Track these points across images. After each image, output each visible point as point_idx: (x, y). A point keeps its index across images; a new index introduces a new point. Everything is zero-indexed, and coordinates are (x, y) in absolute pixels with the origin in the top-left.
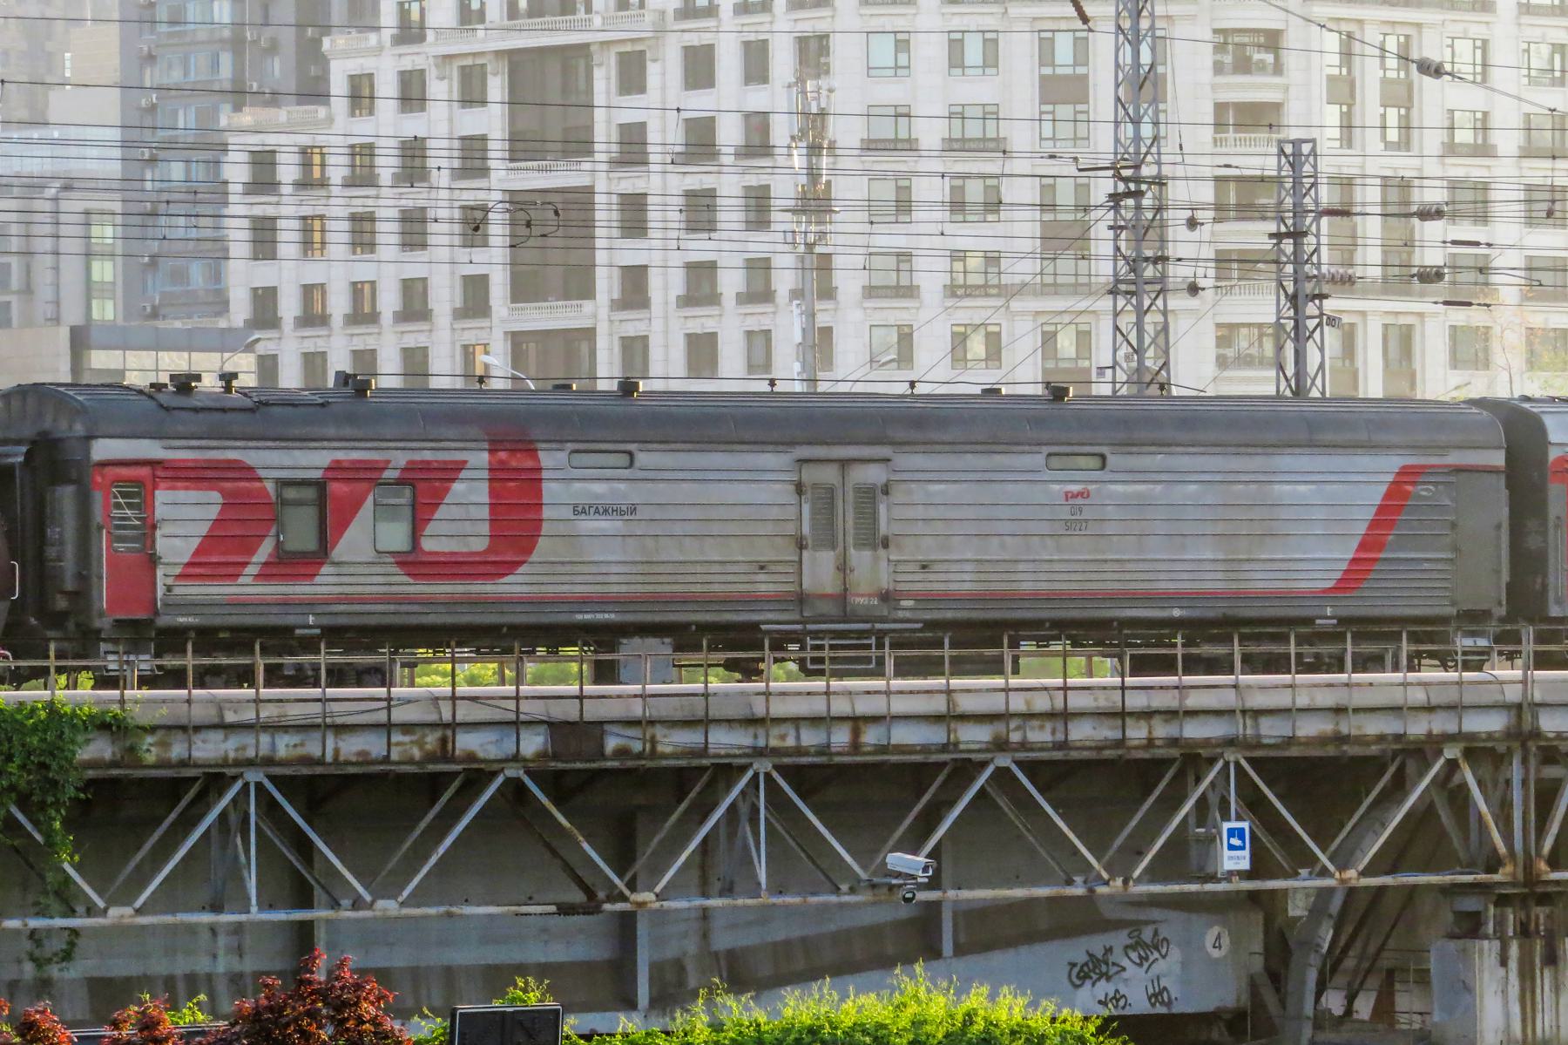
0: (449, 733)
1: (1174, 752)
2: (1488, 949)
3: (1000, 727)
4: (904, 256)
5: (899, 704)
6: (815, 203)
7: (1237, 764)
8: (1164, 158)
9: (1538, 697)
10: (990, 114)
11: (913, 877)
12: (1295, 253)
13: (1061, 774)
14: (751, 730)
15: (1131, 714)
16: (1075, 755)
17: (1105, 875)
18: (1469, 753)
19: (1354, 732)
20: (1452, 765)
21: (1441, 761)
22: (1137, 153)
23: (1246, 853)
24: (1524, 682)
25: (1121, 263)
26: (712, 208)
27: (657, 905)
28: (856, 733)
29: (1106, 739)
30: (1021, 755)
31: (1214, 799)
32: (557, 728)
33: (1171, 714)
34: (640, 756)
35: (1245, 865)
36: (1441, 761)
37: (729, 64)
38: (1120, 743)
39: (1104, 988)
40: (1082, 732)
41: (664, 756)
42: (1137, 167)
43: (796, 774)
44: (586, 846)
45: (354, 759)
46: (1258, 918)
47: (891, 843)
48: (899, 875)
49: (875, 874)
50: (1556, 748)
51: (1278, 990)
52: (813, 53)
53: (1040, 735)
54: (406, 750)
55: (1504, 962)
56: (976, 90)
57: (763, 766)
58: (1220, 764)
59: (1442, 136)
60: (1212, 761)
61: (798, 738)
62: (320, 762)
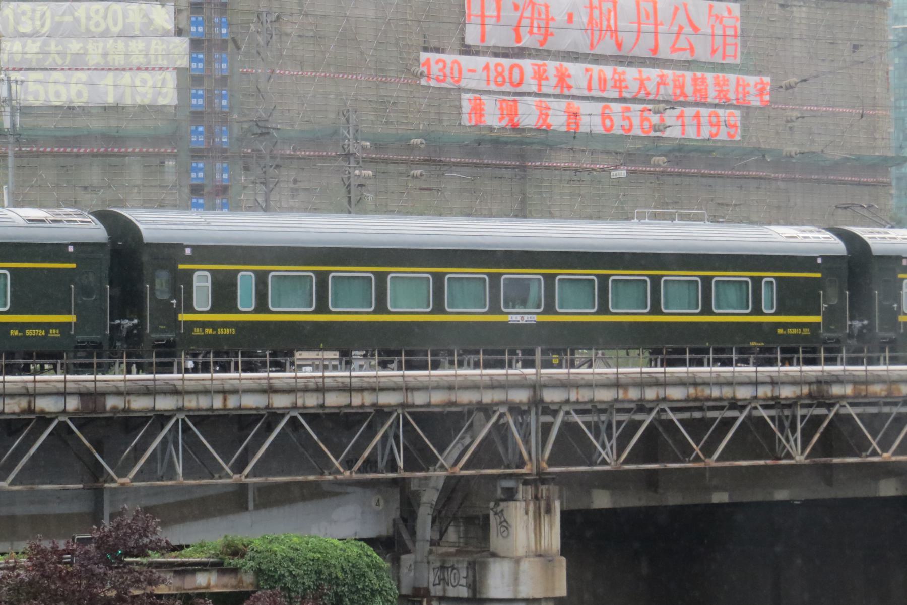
0: (32, 399)
1: (372, 410)
2: (521, 505)
5: (241, 387)
14: (176, 397)
16: (327, 411)
17: (341, 470)
20: (502, 416)
24: (536, 374)
28: (225, 400)
30: (301, 411)
32: (83, 395)
33: (373, 389)
34: (124, 410)
38: (349, 406)
40: (333, 400)
46: (398, 490)
50: (548, 408)
51: (406, 526)
53: (311, 401)
55: (527, 513)
57: (181, 416)
58: (395, 415)
60: (390, 414)
61: (197, 402)
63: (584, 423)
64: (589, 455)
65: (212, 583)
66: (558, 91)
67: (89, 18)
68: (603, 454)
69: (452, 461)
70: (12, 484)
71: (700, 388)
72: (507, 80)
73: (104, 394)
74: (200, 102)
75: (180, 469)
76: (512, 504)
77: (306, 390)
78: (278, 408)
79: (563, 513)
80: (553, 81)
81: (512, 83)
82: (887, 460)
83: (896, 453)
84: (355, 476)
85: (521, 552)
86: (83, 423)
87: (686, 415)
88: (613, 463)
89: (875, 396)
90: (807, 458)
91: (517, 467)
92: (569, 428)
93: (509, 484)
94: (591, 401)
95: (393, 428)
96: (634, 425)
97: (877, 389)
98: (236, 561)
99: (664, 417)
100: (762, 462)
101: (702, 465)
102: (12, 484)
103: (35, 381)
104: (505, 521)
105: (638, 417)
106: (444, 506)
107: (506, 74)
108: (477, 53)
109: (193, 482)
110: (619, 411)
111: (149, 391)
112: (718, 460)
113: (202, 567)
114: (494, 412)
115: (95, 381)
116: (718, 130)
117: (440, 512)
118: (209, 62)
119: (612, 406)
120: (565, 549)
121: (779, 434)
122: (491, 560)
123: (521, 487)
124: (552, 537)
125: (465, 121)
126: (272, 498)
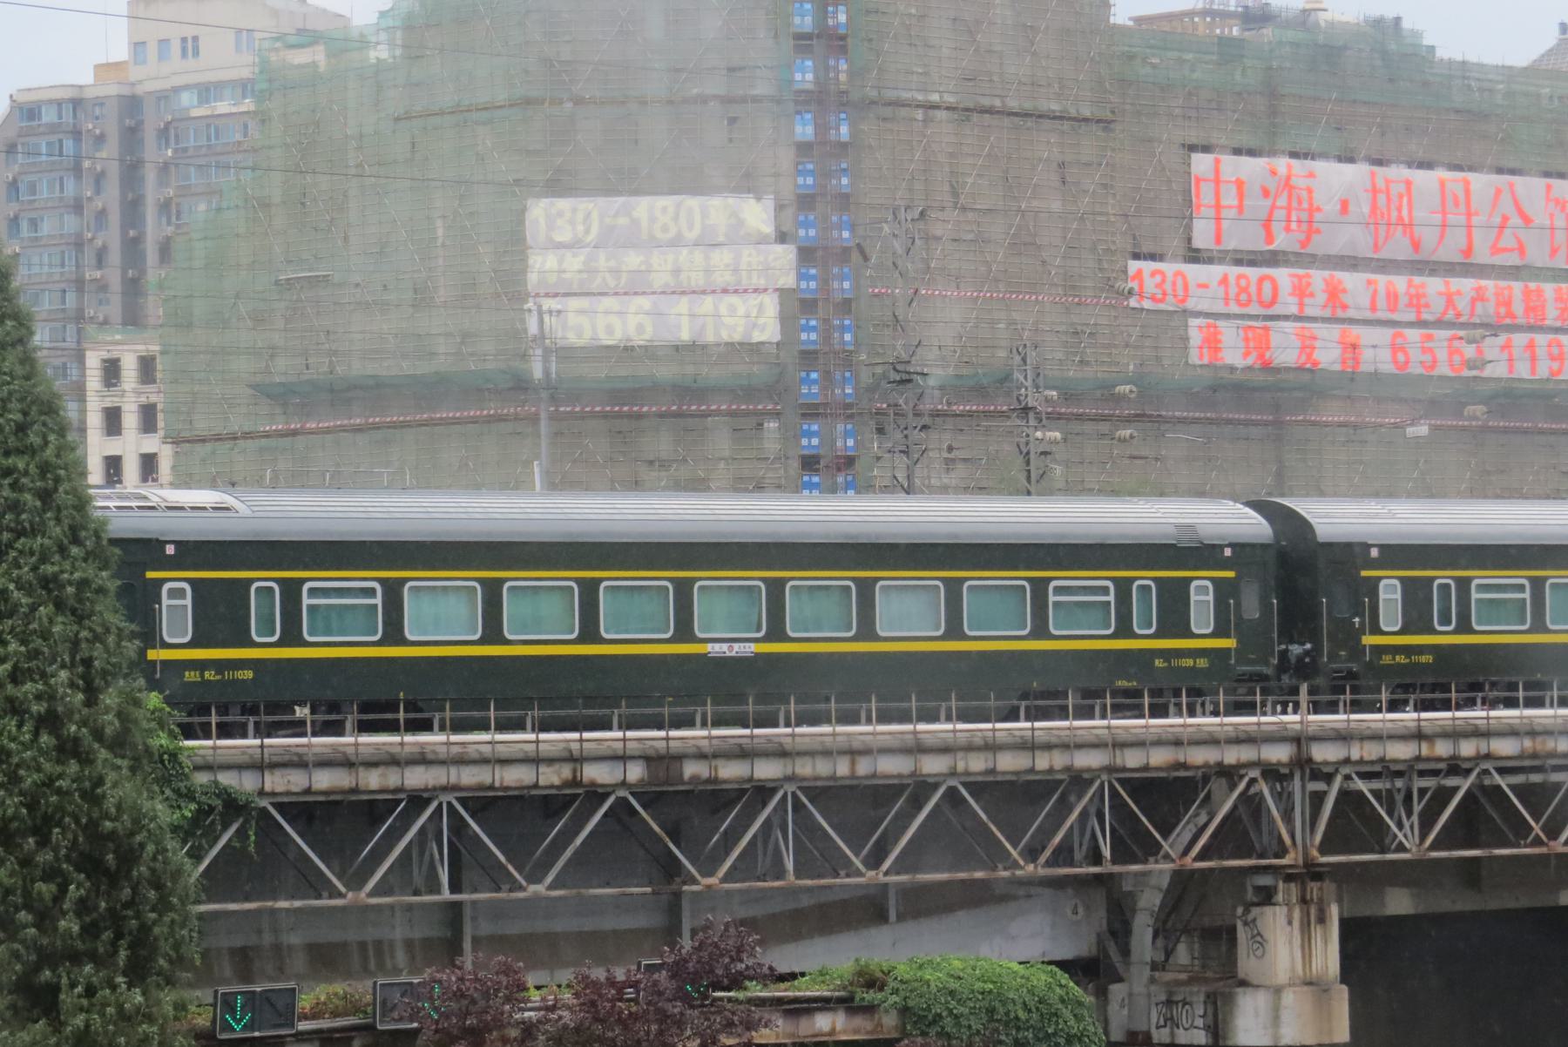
5: (875, 744)
13: (989, 788)
16: (999, 778)
17: (1022, 863)
20: (1253, 781)
21: (1246, 780)
28: (853, 763)
30: (963, 779)
32: (651, 759)
33: (1065, 747)
34: (709, 781)
36: (1246, 780)
38: (1032, 770)
40: (1008, 763)
41: (725, 782)
45: (513, 785)
53: (977, 764)
54: (551, 777)
55: (1290, 923)
57: (790, 788)
58: (1097, 784)
60: (1091, 782)
61: (814, 767)
62: (491, 787)
63: (1372, 791)
64: (1378, 837)
65: (839, 1027)
66: (1327, 313)
67: (652, 220)
68: (1400, 836)
69: (1181, 848)
70: (550, 888)
71: (1539, 739)
72: (1254, 297)
73: (680, 758)
74: (813, 336)
75: (790, 865)
76: (1268, 910)
77: (970, 748)
78: (929, 775)
79: (1344, 923)
80: (1321, 298)
81: (1261, 303)
84: (1042, 872)
85: (1282, 977)
86: (651, 799)
87: (1519, 779)
91: (1277, 856)
92: (1349, 799)
93: (1265, 880)
94: (1382, 760)
95: (1096, 800)
96: (1443, 796)
98: (871, 996)
99: (1487, 782)
101: (1544, 850)
102: (550, 888)
103: (581, 740)
104: (1259, 934)
105: (1450, 782)
106: (1169, 915)
107: (1253, 290)
108: (1210, 261)
109: (809, 882)
110: (1422, 774)
111: (744, 753)
113: (825, 1004)
114: (1242, 777)
115: (667, 739)
116: (1562, 364)
117: (1165, 922)
118: (825, 281)
119: (1411, 767)
122: (1240, 990)
123: (1281, 885)
124: (1328, 956)
125: (1194, 359)
126: (923, 904)
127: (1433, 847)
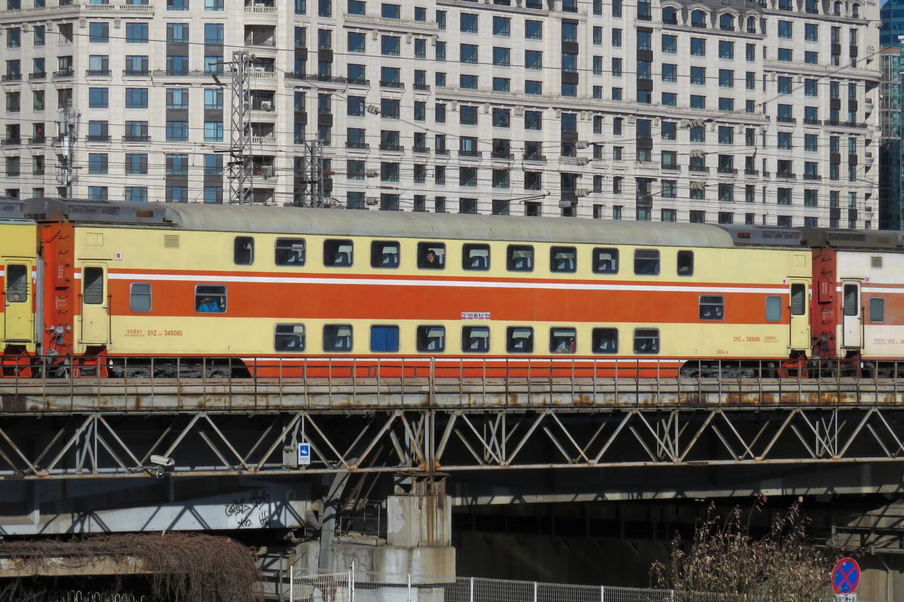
1: (277, 412)
3: (201, 399)
4: (106, 188)
6: (65, 162)
7: (305, 417)
8: (253, 147)
9: (436, 389)
10: (144, 125)
11: (163, 466)
12: (312, 190)
13: (227, 420)
14: (92, 399)
15: (259, 394)
16: (233, 412)
18: (406, 414)
19: (356, 403)
20: (399, 419)
22: (241, 144)
23: (309, 457)
25: (233, 193)
26: (18, 166)
27: (48, 477)
28: (138, 401)
29: (248, 406)
31: (295, 434)
32: (5, 396)
35: (308, 462)
37: (27, 101)
38: (255, 408)
39: (241, 517)
40: (238, 402)
42: (241, 151)
43: (108, 418)
44: (18, 451)
47: (152, 450)
48: (157, 465)
49: (144, 464)
52: (65, 96)
56: (137, 115)
57: (98, 415)
59: (345, 139)
60: (293, 416)
71: (584, 395)
76: (406, 499)
79: (454, 508)
82: (759, 462)
83: (766, 457)
85: (414, 543)
88: (503, 463)
89: (749, 404)
90: (683, 461)
97: (751, 398)
100: (641, 464)
101: (586, 465)
112: (599, 462)
120: (456, 541)
121: (659, 440)
123: (415, 484)
124: (444, 529)
127: (511, 464)
